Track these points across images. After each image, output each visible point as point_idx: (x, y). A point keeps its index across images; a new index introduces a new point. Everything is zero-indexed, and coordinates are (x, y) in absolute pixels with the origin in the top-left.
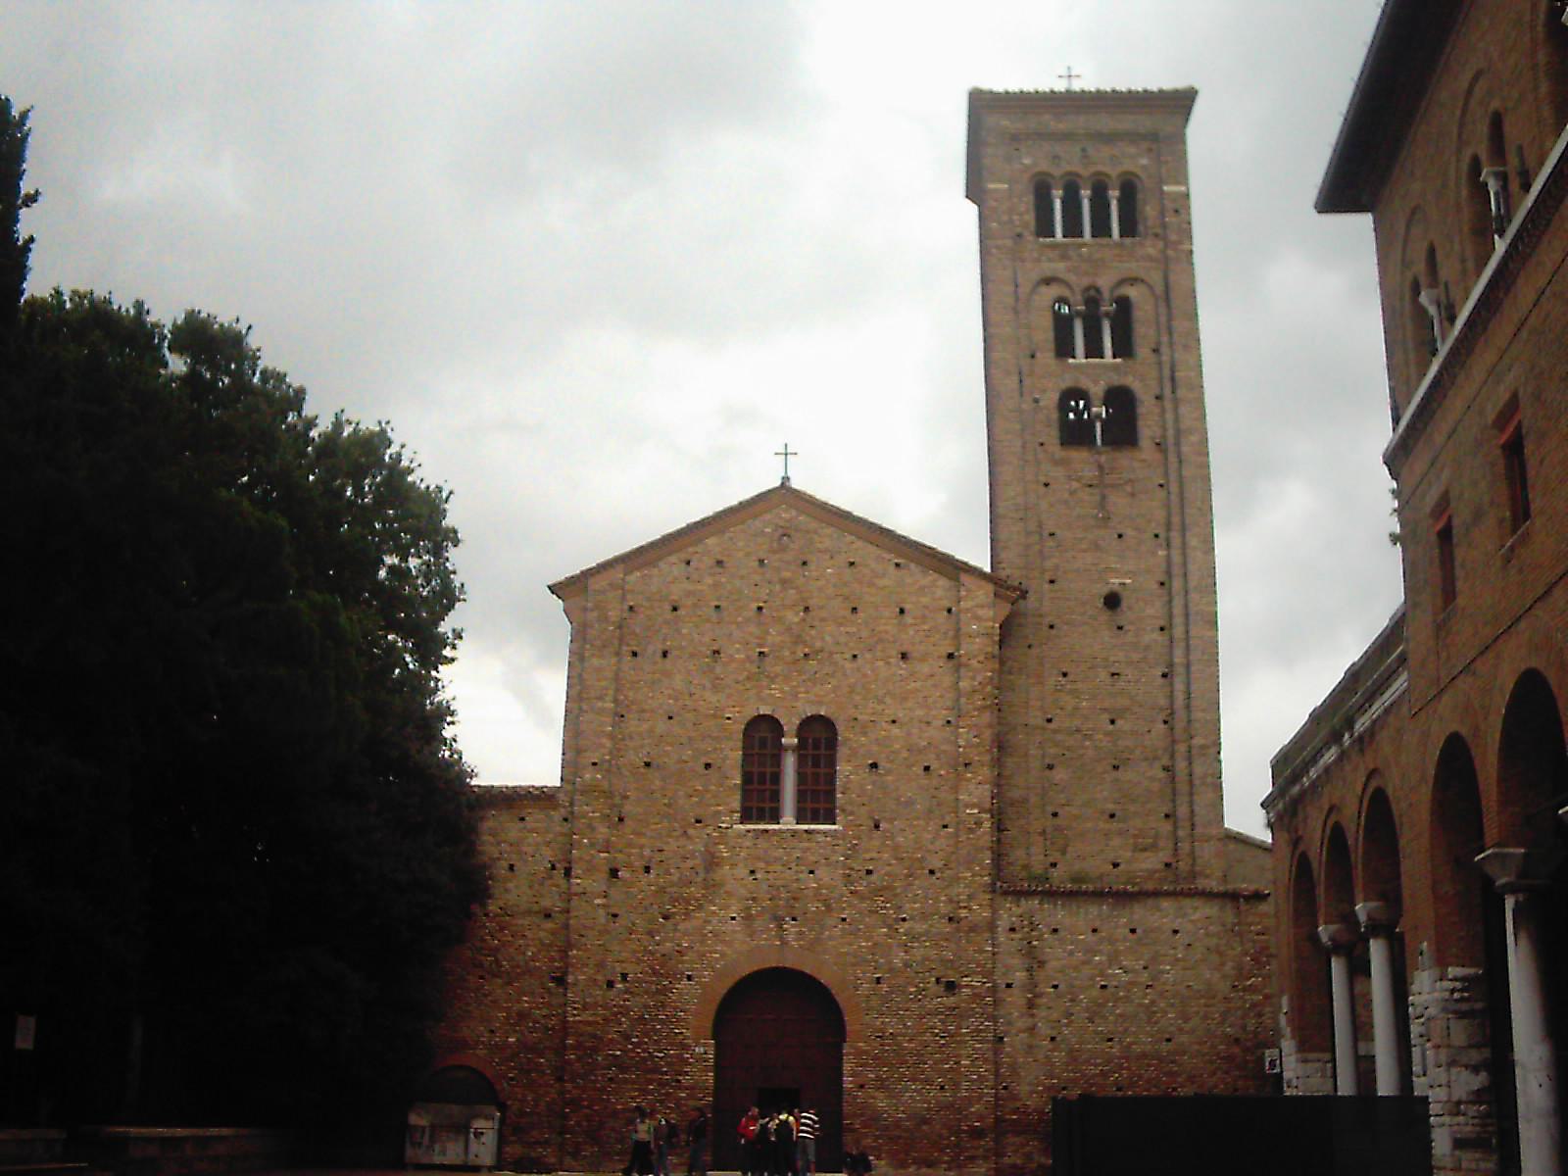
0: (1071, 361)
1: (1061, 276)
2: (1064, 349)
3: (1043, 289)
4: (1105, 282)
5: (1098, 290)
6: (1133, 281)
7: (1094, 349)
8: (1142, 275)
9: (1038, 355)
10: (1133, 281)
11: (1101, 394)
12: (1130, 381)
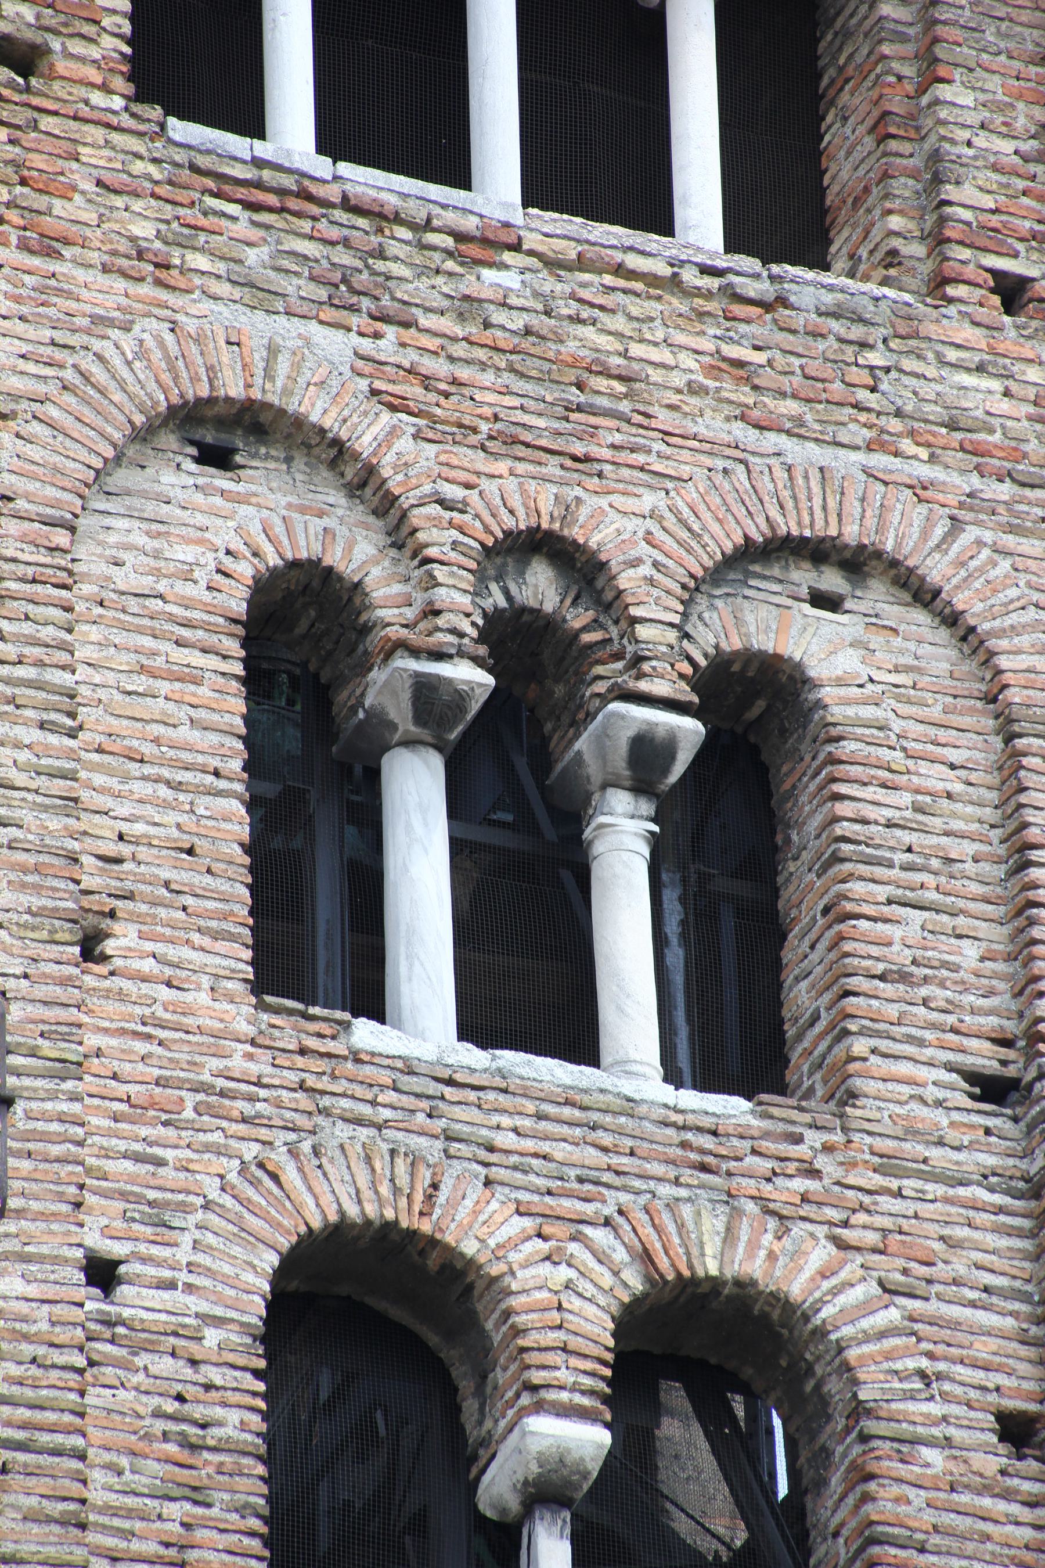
0: (365, 1033)
1: (318, 410)
2: (313, 938)
3: (176, 476)
4: (611, 524)
5: (583, 570)
6: (841, 564)
7: (528, 983)
8: (904, 531)
9: (122, 940)
10: (841, 564)
11: (595, 1325)
12: (795, 1268)
